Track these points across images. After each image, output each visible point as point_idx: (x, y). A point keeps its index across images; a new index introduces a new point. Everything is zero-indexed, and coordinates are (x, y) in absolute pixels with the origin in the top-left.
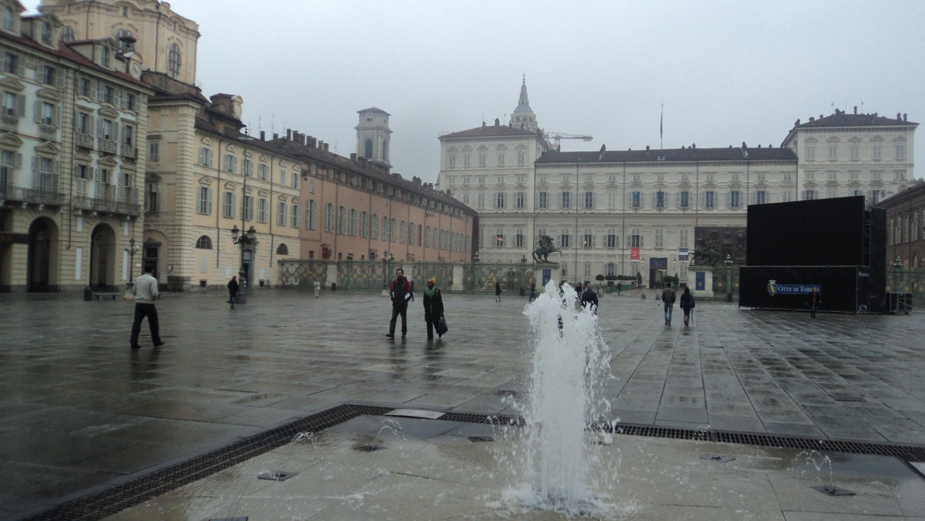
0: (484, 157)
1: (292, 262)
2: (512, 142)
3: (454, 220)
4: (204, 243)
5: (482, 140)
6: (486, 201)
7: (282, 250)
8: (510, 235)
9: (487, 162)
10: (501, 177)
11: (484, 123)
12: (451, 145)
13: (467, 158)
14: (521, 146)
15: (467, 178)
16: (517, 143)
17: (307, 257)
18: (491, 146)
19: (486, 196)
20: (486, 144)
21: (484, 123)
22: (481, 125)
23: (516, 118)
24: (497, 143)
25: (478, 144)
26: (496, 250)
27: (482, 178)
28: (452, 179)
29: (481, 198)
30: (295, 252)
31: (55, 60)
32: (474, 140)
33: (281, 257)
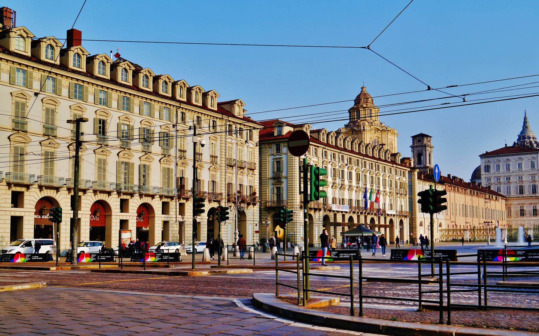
0: (509, 165)
1: (445, 230)
2: (527, 156)
3: (497, 202)
4: (421, 225)
5: (507, 155)
6: (512, 190)
7: (440, 226)
8: (528, 209)
9: (511, 168)
10: (521, 178)
11: (506, 145)
12: (487, 159)
13: (498, 167)
14: (533, 158)
15: (498, 178)
16: (530, 156)
17: (447, 228)
18: (513, 160)
19: (511, 188)
20: (509, 158)
21: (506, 145)
22: (504, 146)
23: (522, 136)
24: (516, 157)
25: (505, 158)
26: (520, 218)
27: (508, 179)
28: (489, 179)
29: (509, 189)
30: (444, 227)
31: (391, 165)
32: (502, 156)
33: (440, 228)
